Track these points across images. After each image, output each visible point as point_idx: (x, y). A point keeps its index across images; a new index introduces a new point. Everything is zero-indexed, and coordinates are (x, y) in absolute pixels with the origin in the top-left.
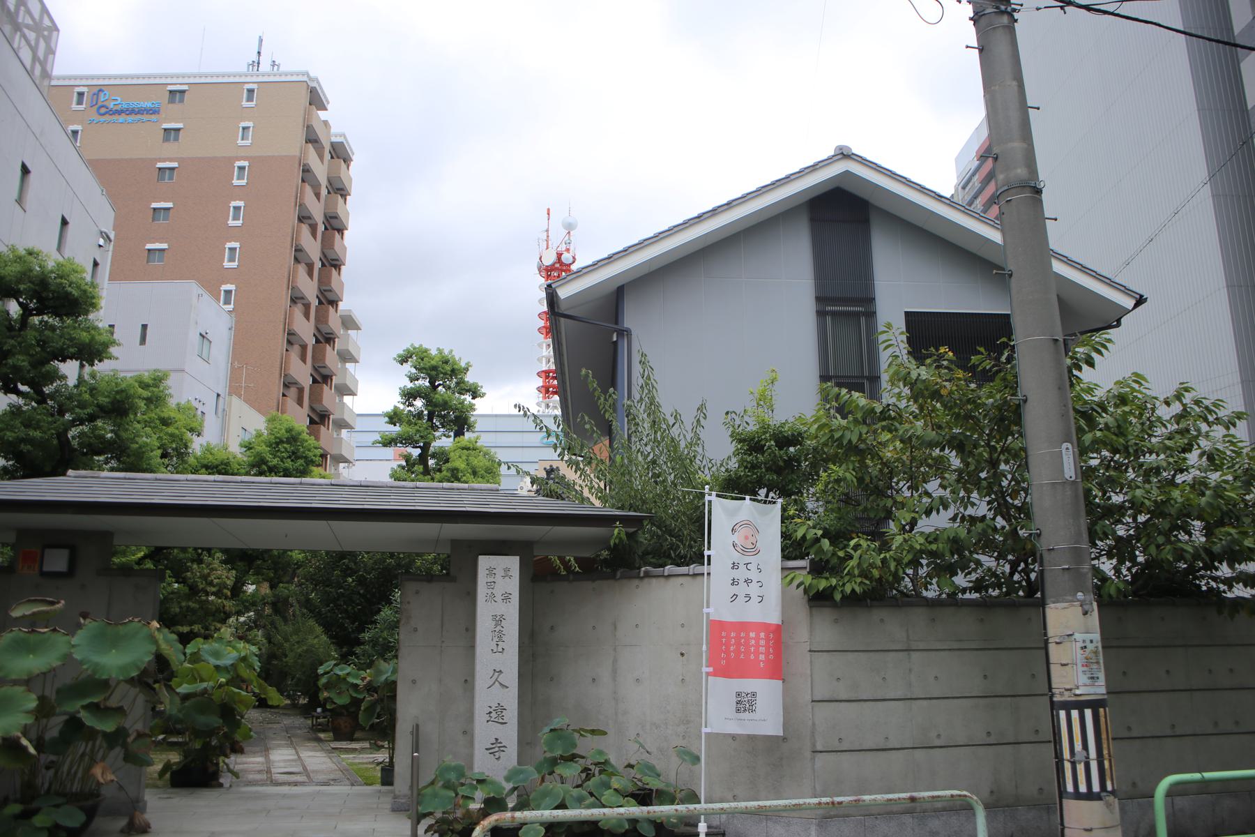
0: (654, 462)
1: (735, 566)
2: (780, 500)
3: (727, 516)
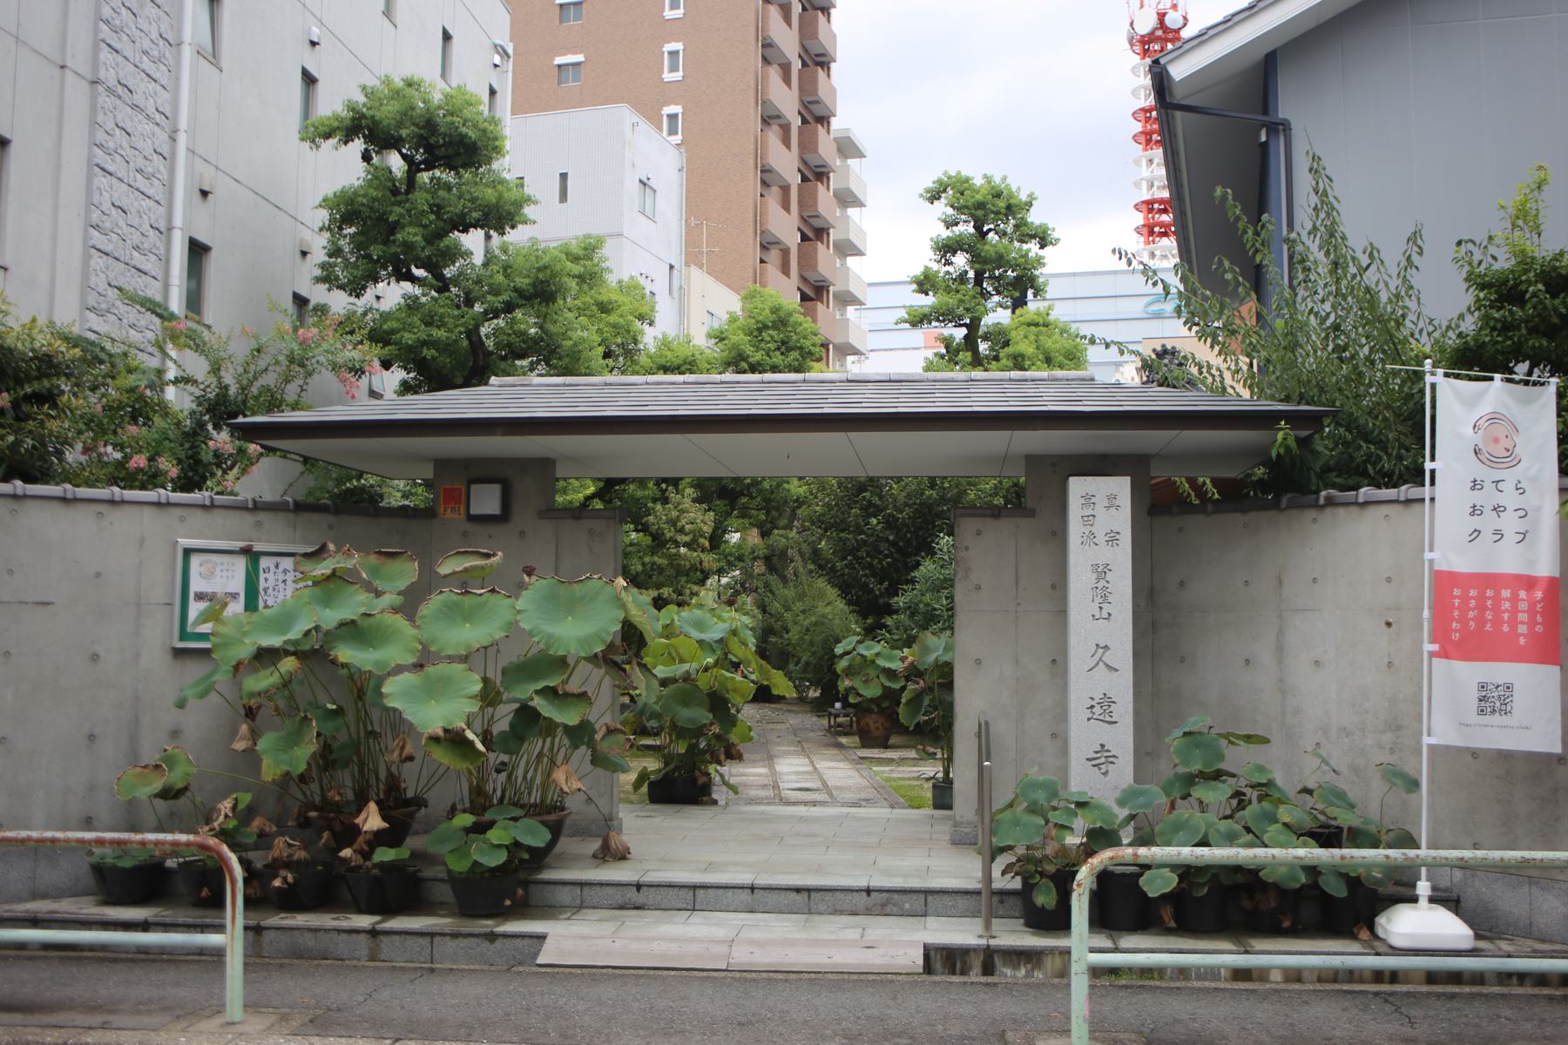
0: (1336, 327)
1: (1475, 485)
2: (1554, 380)
3: (1463, 409)
